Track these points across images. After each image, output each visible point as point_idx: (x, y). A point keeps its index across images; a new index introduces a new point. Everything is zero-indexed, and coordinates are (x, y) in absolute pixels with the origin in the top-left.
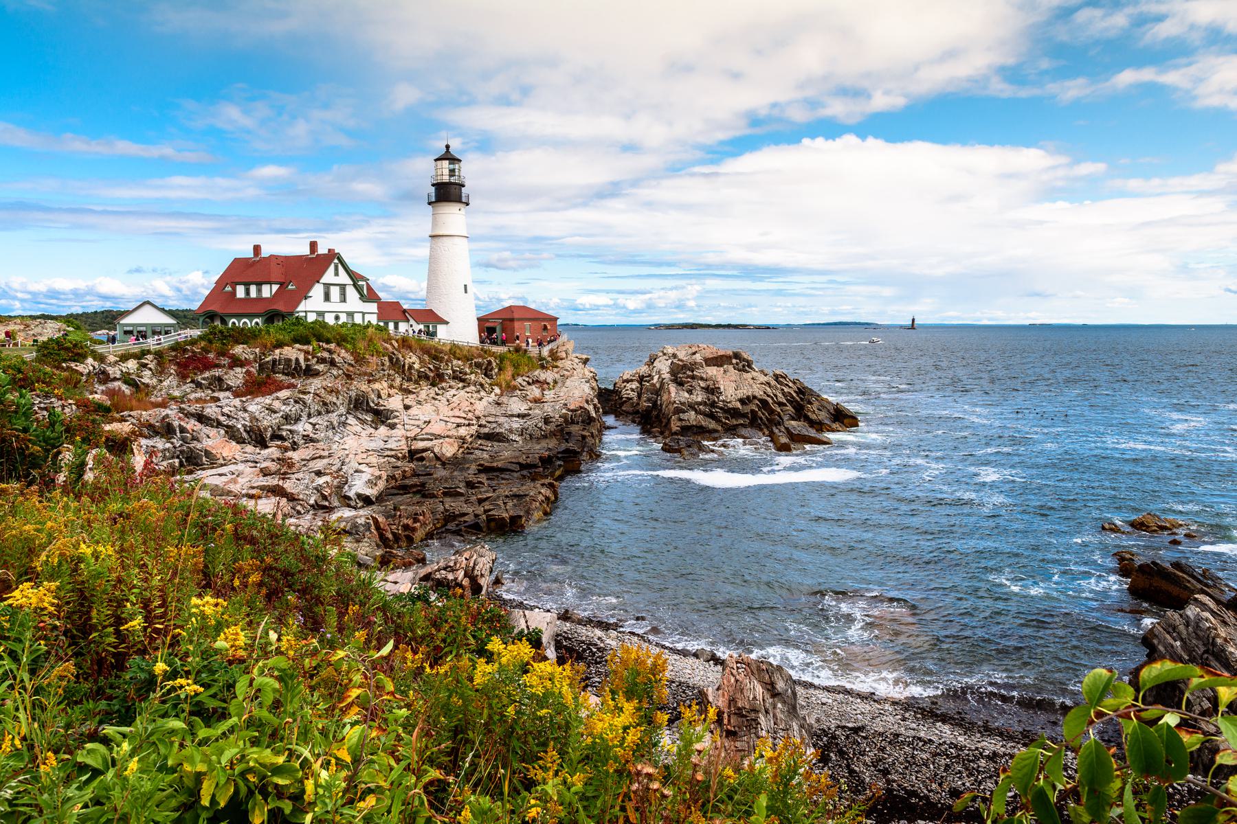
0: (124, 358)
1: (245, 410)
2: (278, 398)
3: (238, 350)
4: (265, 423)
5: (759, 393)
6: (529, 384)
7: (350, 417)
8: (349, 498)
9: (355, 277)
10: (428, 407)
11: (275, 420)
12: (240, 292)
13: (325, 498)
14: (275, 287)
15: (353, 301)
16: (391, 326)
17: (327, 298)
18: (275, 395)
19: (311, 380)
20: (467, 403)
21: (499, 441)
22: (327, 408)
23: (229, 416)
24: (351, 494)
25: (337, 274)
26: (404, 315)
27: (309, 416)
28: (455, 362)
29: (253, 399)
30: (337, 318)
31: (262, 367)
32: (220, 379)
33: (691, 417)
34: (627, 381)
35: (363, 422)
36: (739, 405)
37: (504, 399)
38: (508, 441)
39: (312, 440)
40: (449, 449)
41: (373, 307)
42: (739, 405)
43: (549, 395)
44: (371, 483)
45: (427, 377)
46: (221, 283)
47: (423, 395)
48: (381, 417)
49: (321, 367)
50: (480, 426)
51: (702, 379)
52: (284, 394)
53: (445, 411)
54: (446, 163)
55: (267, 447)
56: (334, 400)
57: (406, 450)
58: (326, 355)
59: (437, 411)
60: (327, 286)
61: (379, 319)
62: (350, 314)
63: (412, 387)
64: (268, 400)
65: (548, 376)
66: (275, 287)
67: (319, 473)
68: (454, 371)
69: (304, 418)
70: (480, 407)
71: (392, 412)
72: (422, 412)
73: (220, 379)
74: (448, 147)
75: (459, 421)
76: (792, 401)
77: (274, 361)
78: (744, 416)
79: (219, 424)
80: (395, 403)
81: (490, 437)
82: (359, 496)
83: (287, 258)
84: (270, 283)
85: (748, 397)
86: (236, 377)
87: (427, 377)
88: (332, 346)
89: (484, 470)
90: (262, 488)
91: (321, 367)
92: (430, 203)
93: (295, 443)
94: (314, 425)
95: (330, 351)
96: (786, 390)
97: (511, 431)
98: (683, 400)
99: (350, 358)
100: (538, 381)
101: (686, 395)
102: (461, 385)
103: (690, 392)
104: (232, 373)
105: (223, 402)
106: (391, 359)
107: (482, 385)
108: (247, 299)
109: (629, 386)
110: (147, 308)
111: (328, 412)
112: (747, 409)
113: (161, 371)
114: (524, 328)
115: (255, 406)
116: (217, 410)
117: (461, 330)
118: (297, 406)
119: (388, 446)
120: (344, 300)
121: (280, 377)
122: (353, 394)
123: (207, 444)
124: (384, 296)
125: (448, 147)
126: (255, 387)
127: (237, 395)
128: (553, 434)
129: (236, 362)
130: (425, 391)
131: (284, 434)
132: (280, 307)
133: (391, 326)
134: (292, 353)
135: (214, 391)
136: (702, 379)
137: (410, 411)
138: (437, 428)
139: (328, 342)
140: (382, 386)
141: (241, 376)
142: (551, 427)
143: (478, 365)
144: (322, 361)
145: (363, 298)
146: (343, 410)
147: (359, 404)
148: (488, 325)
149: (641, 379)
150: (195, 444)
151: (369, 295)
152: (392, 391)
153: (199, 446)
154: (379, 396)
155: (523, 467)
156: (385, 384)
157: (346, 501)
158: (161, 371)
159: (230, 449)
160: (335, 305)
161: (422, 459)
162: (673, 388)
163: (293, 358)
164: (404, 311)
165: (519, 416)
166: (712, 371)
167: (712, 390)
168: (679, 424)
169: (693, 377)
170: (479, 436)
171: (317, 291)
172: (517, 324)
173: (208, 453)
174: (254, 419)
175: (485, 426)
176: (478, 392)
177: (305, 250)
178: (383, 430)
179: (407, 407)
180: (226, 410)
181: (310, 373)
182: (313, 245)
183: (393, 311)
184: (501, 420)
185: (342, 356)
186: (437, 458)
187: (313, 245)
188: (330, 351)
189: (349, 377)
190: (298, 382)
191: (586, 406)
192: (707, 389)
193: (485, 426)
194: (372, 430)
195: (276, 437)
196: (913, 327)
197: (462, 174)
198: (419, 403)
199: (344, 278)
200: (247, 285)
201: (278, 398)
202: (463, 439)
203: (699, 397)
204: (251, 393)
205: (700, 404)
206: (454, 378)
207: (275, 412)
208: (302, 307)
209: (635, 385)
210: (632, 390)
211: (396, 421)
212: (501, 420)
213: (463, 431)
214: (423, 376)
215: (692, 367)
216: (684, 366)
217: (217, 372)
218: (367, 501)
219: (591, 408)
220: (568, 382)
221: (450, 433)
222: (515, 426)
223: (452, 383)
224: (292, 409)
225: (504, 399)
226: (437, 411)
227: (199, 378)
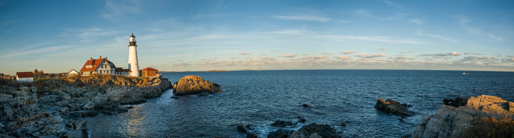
9: (109, 62)
24: (84, 107)
41: (114, 69)
62: (108, 71)
120: (106, 67)
138: (115, 95)
170: (125, 96)
174: (77, 92)
177: (99, 58)
218: (87, 109)
224: (85, 90)
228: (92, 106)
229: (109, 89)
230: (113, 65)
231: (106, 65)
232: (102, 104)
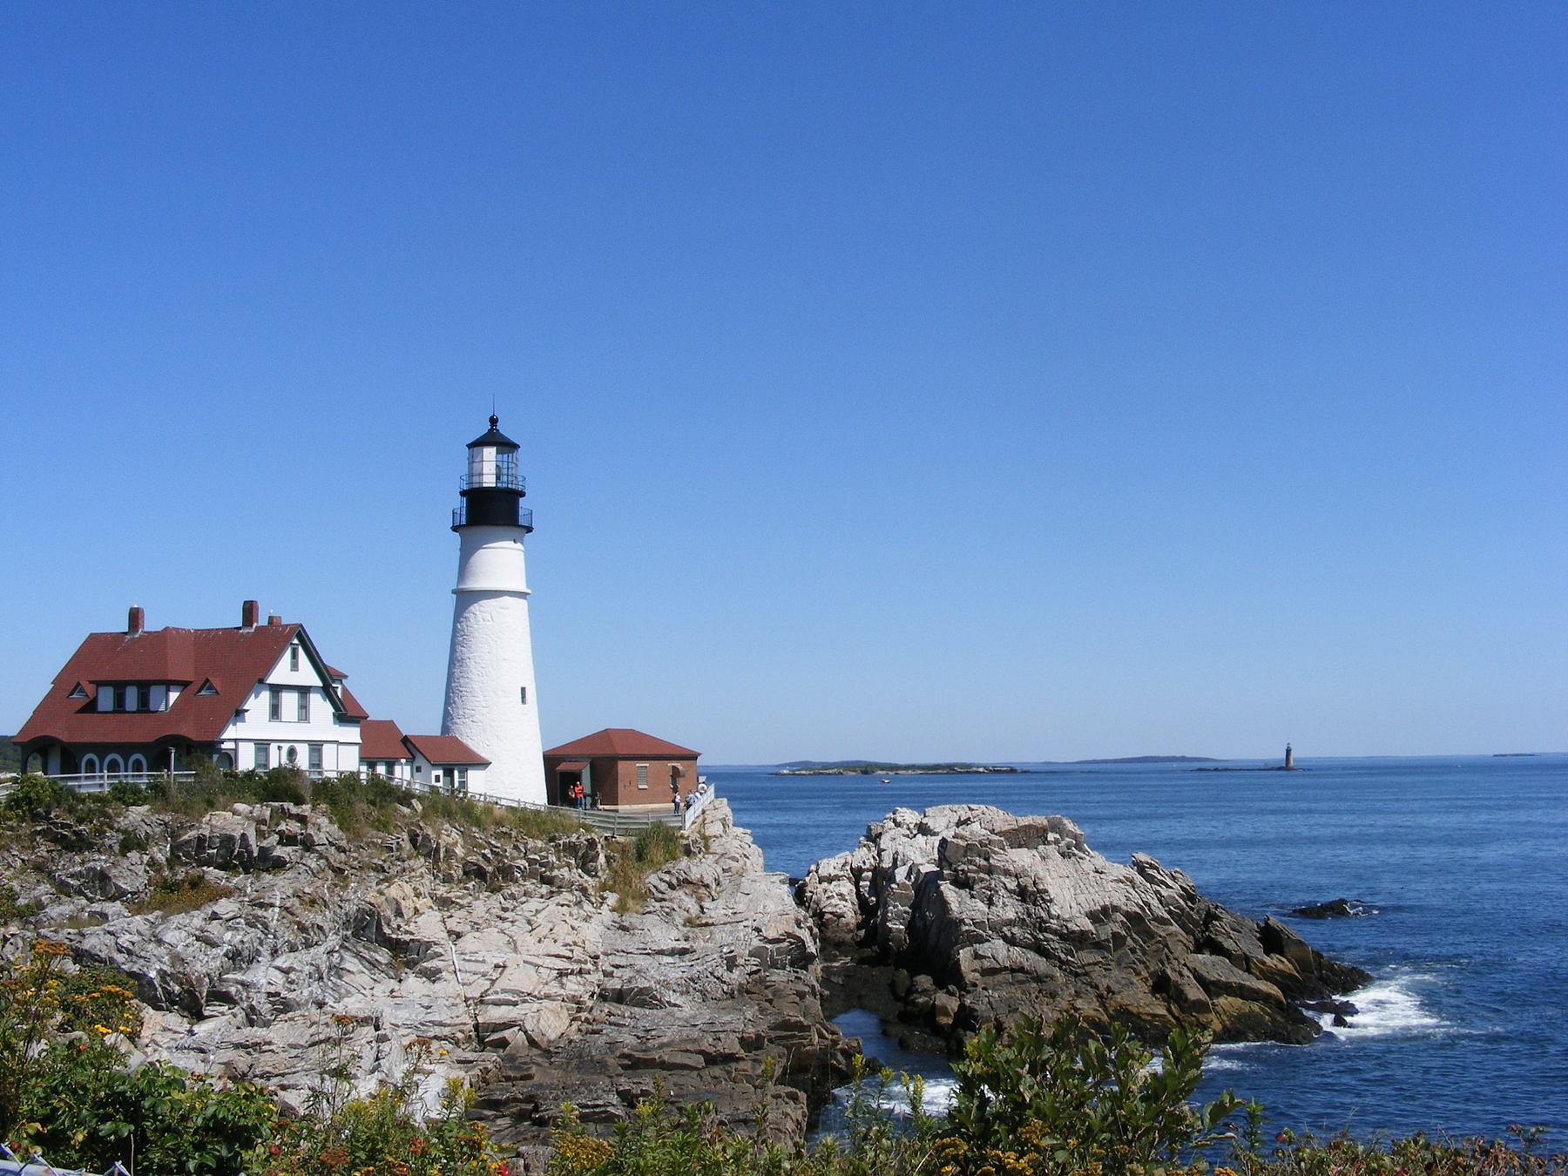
1: (160, 942)
2: (215, 916)
4: (198, 967)
5: (1118, 899)
6: (672, 887)
7: (347, 955)
10: (492, 934)
14: (174, 696)
17: (275, 712)
18: (209, 909)
19: (267, 877)
20: (567, 928)
21: (642, 1004)
22: (308, 936)
23: (130, 952)
25: (295, 667)
26: (411, 748)
27: (275, 952)
28: (531, 844)
29: (164, 918)
30: (292, 753)
32: (103, 877)
33: (997, 949)
34: (830, 879)
35: (374, 964)
36: (1087, 925)
37: (630, 919)
38: (661, 1005)
40: (553, 1023)
42: (1087, 925)
43: (716, 910)
45: (480, 874)
46: (67, 683)
48: (407, 955)
50: (607, 974)
51: (1007, 873)
52: (225, 907)
53: (527, 942)
54: (490, 453)
55: (199, 1017)
56: (319, 920)
57: (471, 1022)
58: (294, 827)
59: (513, 945)
60: (276, 690)
61: (362, 760)
62: (316, 747)
63: (456, 893)
64: (197, 919)
66: (174, 696)
68: (531, 862)
69: (265, 951)
71: (428, 945)
72: (486, 946)
73: (103, 877)
74: (493, 421)
75: (561, 964)
76: (1180, 917)
77: (201, 840)
78: (1099, 946)
80: (428, 926)
81: (620, 997)
83: (199, 634)
84: (169, 684)
85: (1104, 909)
86: (132, 873)
87: (480, 874)
88: (306, 809)
89: (635, 1064)
92: (455, 529)
93: (252, 1008)
94: (286, 972)
95: (302, 819)
96: (1165, 892)
97: (666, 985)
98: (979, 917)
100: (688, 882)
101: (982, 906)
102: (545, 889)
103: (990, 903)
104: (126, 863)
105: (116, 924)
106: (413, 839)
107: (584, 890)
109: (833, 887)
111: (308, 945)
115: (179, 931)
116: (109, 939)
117: (513, 777)
118: (255, 933)
119: (437, 1018)
121: (212, 873)
122: (351, 908)
124: (373, 716)
125: (493, 421)
127: (137, 905)
128: (745, 990)
129: (131, 842)
130: (484, 904)
131: (233, 990)
132: (188, 731)
134: (233, 819)
135: (91, 900)
136: (1007, 873)
137: (469, 943)
139: (299, 801)
140: (398, 890)
141: (140, 869)
142: (736, 976)
143: (571, 849)
144: (287, 840)
146: (333, 941)
147: (366, 928)
148: (563, 767)
149: (857, 874)
152: (420, 903)
154: (399, 913)
155: (711, 1060)
156: (408, 889)
160: (289, 729)
161: (503, 1043)
162: (947, 889)
163: (237, 835)
164: (406, 740)
165: (672, 953)
166: (1021, 858)
167: (1029, 894)
168: (977, 964)
169: (990, 870)
171: (258, 704)
172: (622, 766)
174: (177, 959)
175: (611, 975)
176: (579, 903)
178: (413, 984)
180: (124, 940)
182: (249, 610)
183: (386, 743)
184: (642, 962)
186: (532, 1042)
187: (249, 610)
188: (302, 819)
189: (338, 871)
191: (799, 932)
192: (1022, 894)
193: (611, 975)
194: (393, 984)
196: (1286, 767)
197: (522, 471)
198: (476, 926)
199: (307, 675)
200: (119, 687)
201: (215, 916)
202: (576, 1000)
203: (1009, 909)
204: (161, 906)
205: (1010, 923)
206: (532, 875)
207: (213, 945)
208: (231, 732)
209: (847, 887)
210: (842, 896)
211: (435, 963)
212: (642, 962)
213: (573, 986)
215: (982, 849)
216: (969, 848)
217: (100, 861)
219: (805, 935)
220: (746, 884)
221: (546, 990)
222: (674, 975)
223: (529, 885)
225: (630, 919)
226: (513, 945)
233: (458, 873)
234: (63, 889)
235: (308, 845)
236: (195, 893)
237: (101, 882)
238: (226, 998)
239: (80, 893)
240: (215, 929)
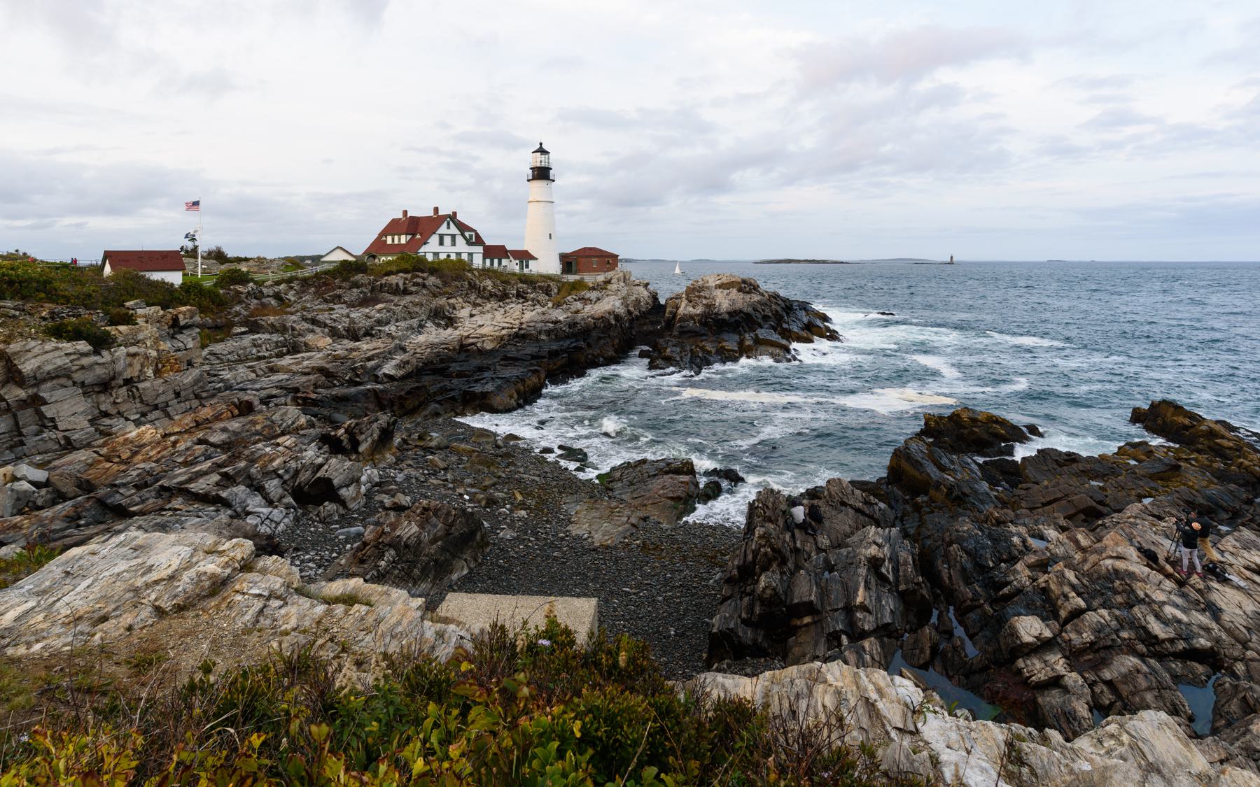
0: (278, 283)
1: (348, 316)
3: (359, 277)
8: (377, 377)
9: (462, 228)
10: (490, 315)
11: (367, 323)
12: (389, 241)
13: (358, 376)
14: (409, 237)
15: (461, 246)
16: (496, 261)
17: (441, 243)
22: (411, 315)
24: (380, 373)
27: (397, 321)
31: (373, 290)
35: (438, 325)
36: (726, 317)
39: (393, 338)
40: (489, 346)
41: (480, 249)
43: (588, 308)
44: (399, 367)
45: (496, 296)
47: (489, 306)
48: (451, 322)
49: (414, 289)
56: (417, 309)
58: (419, 280)
62: (459, 254)
65: (593, 295)
66: (409, 237)
67: (369, 359)
70: (528, 316)
72: (479, 320)
73: (340, 297)
79: (326, 325)
80: (464, 313)
82: (385, 375)
88: (425, 275)
90: (313, 368)
91: (414, 289)
95: (424, 279)
99: (438, 282)
106: (470, 283)
108: (393, 245)
110: (339, 251)
112: (733, 320)
113: (300, 293)
114: (592, 263)
122: (433, 306)
123: (309, 338)
126: (364, 302)
129: (356, 285)
133: (496, 261)
139: (423, 272)
144: (416, 284)
145: (469, 243)
146: (423, 317)
150: (302, 339)
151: (479, 241)
153: (302, 339)
157: (376, 379)
158: (300, 293)
159: (325, 341)
164: (507, 251)
169: (699, 297)
170: (516, 335)
171: (434, 240)
173: (306, 344)
174: (353, 321)
178: (450, 330)
179: (472, 316)
181: (406, 292)
185: (432, 280)
190: (396, 299)
194: (441, 330)
195: (368, 333)
198: (482, 313)
199: (454, 230)
200: (393, 235)
202: (502, 338)
203: (699, 310)
214: (492, 295)
217: (338, 292)
218: (391, 378)
224: (384, 315)
226: (493, 319)
227: (326, 296)
228: (409, 368)
229: (464, 313)
230: (478, 236)
231: (453, 236)
232: (442, 361)
233: (487, 294)
234: (326, 301)
235: (424, 286)
236: (376, 301)
237: (338, 299)
238: (372, 336)
239: (332, 301)
240: (373, 313)
